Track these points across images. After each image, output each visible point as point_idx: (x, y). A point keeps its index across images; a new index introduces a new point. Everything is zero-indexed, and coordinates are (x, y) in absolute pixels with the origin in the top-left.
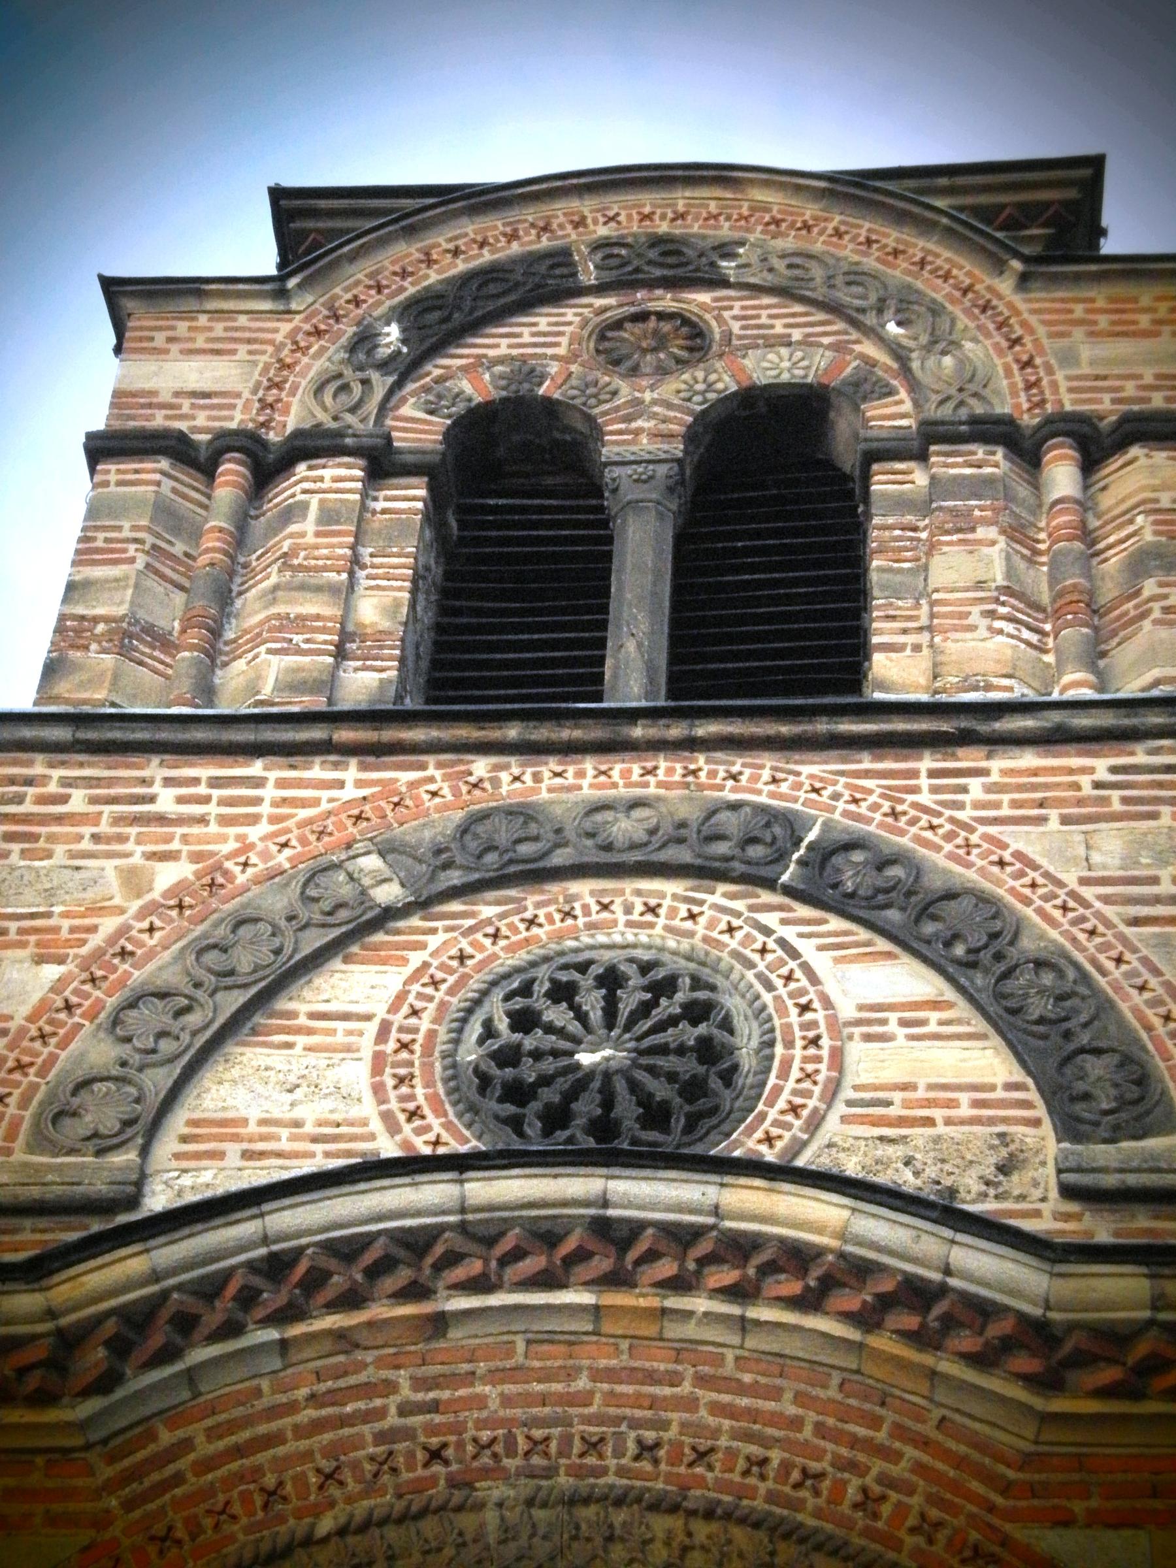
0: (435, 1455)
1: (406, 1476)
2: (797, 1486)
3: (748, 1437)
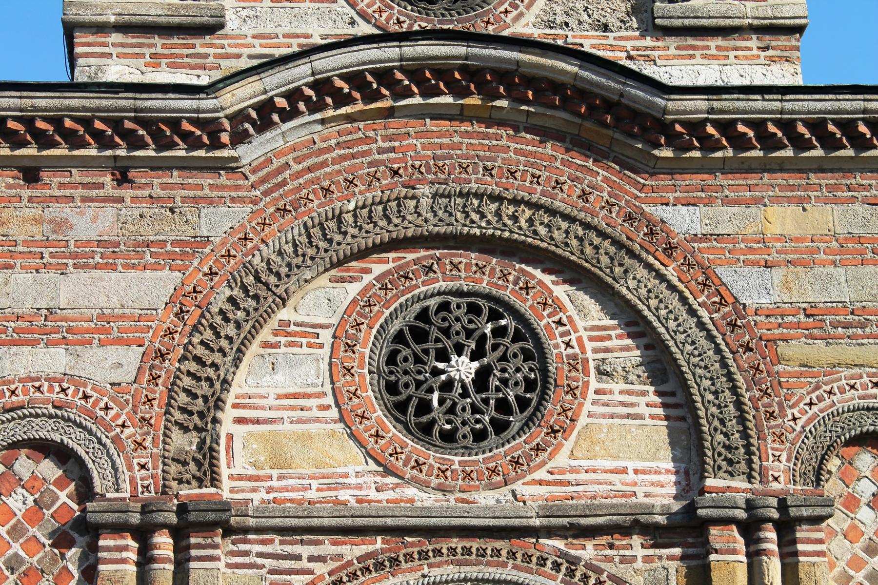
0: (396, 173)
1: (384, 182)
2: (554, 188)
3: (532, 165)
